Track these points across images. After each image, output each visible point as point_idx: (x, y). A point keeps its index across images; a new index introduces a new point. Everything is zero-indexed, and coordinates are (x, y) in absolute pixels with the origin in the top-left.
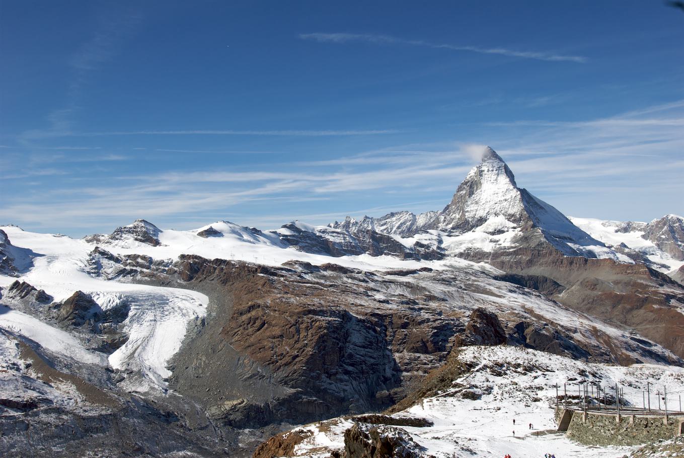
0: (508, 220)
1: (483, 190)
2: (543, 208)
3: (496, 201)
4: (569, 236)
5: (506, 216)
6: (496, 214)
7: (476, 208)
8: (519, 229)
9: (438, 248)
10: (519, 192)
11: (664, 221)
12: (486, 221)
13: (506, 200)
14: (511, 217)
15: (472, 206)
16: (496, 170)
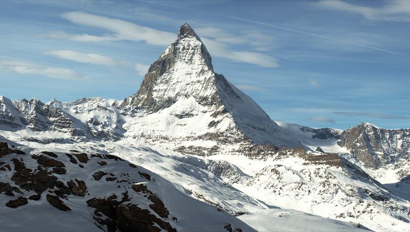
0: (199, 103)
1: (175, 69)
2: (239, 97)
3: (189, 82)
4: (263, 128)
5: (197, 98)
6: (187, 96)
7: (165, 87)
8: (211, 113)
9: (116, 127)
10: (213, 75)
11: (361, 128)
12: (174, 102)
13: (199, 82)
14: (203, 100)
15: (161, 85)
16: (192, 49)
